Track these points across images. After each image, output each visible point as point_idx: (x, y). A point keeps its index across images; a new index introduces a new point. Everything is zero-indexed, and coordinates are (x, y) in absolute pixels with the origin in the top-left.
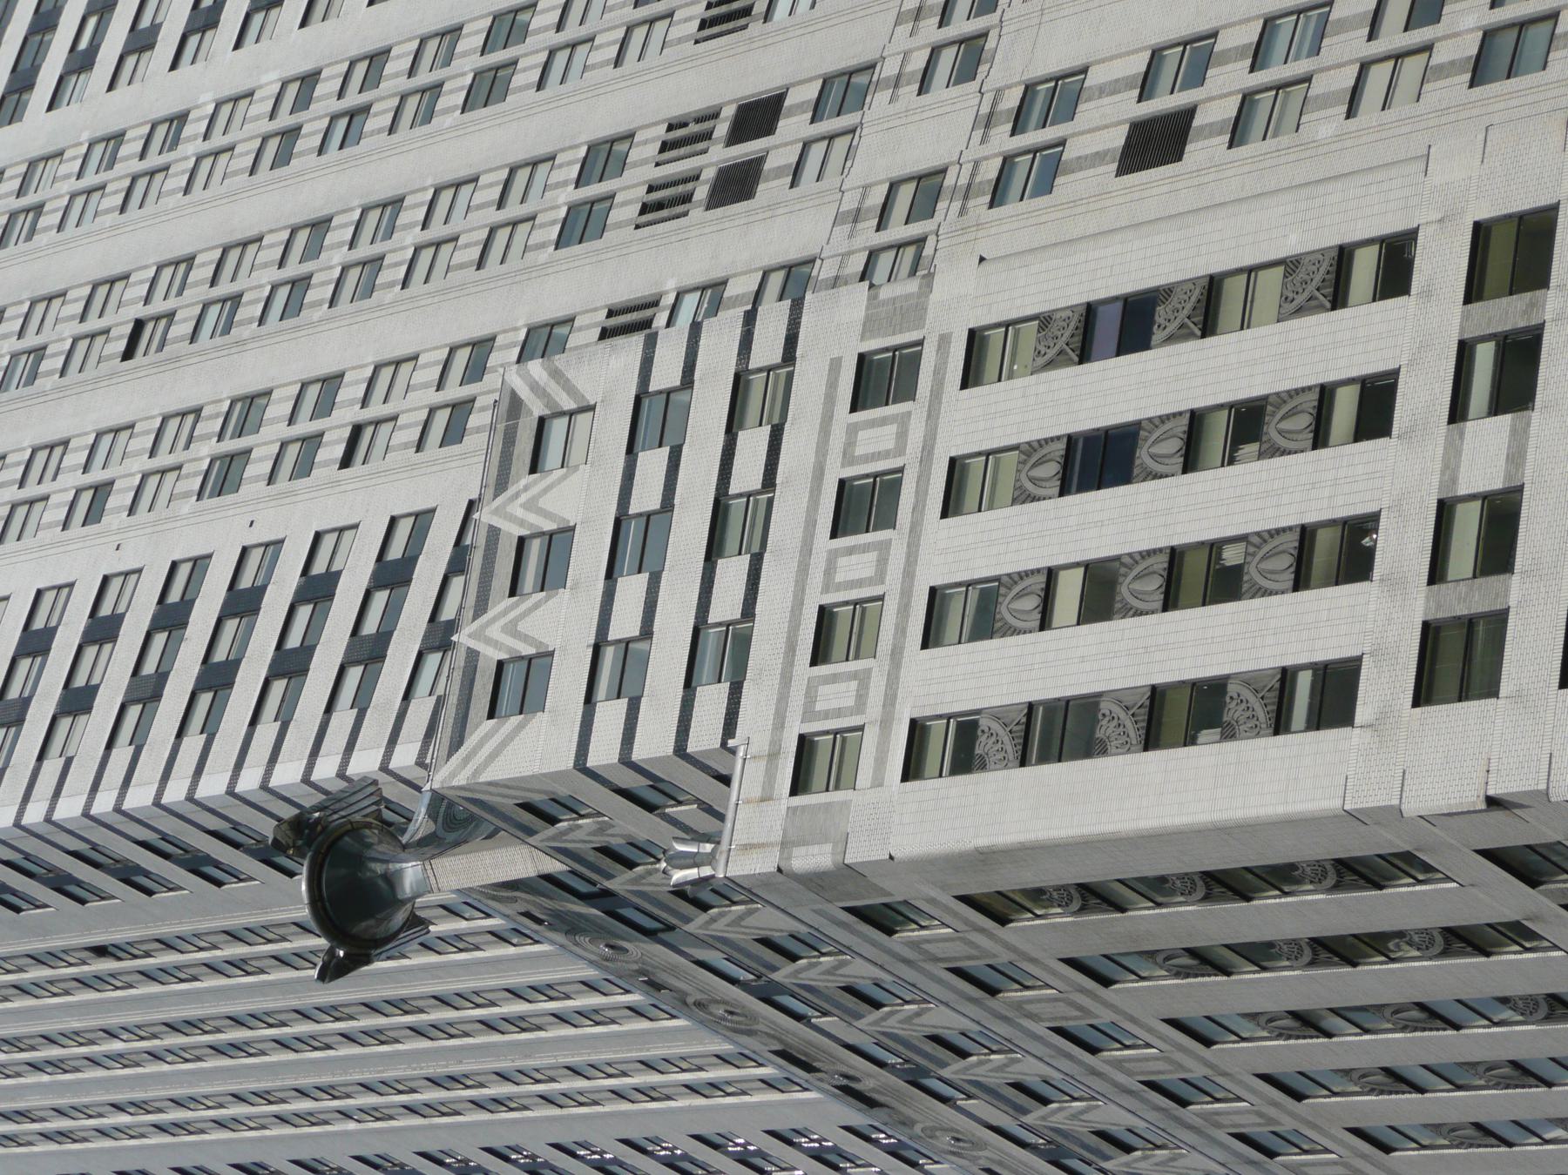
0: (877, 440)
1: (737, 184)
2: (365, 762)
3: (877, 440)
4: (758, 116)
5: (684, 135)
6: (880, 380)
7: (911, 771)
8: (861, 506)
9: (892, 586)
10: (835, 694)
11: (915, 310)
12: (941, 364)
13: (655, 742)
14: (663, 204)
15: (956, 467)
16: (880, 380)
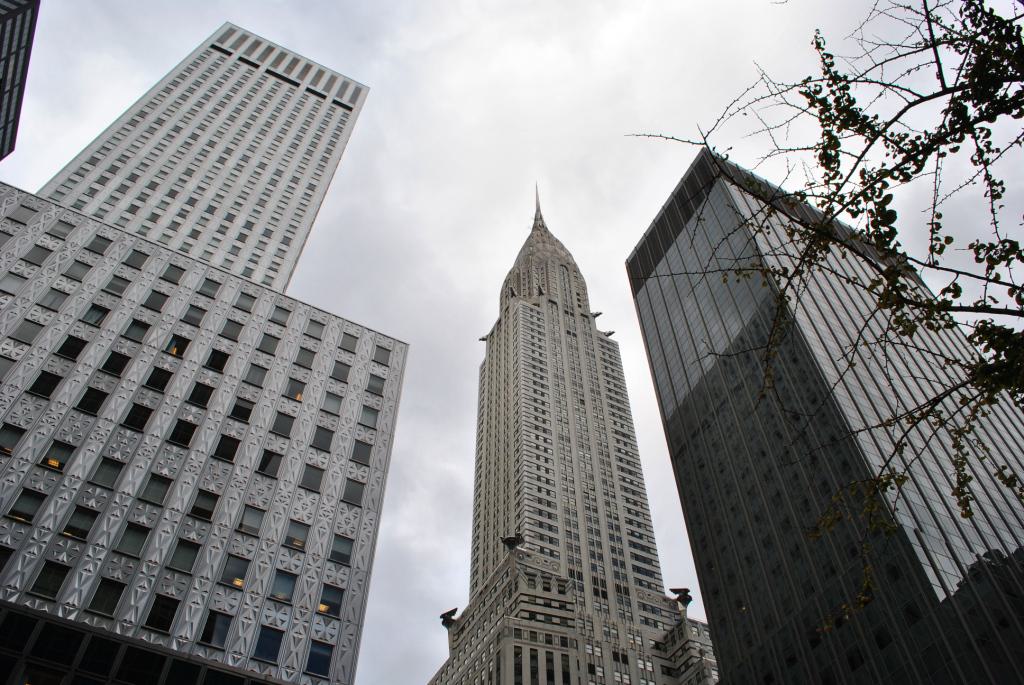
0: (557, 641)
1: (596, 592)
2: (527, 539)
3: (557, 641)
4: (605, 595)
5: (604, 583)
6: (564, 642)
7: (515, 647)
8: (549, 640)
9: (539, 644)
10: (526, 635)
11: (572, 646)
12: (565, 651)
13: (523, 606)
14: (595, 580)
15: (552, 653)
16: (564, 642)
